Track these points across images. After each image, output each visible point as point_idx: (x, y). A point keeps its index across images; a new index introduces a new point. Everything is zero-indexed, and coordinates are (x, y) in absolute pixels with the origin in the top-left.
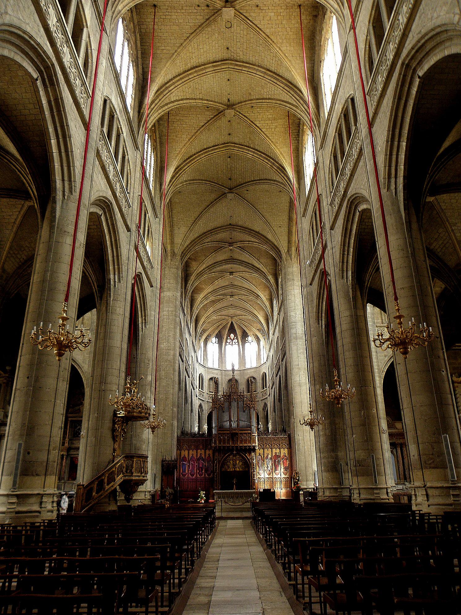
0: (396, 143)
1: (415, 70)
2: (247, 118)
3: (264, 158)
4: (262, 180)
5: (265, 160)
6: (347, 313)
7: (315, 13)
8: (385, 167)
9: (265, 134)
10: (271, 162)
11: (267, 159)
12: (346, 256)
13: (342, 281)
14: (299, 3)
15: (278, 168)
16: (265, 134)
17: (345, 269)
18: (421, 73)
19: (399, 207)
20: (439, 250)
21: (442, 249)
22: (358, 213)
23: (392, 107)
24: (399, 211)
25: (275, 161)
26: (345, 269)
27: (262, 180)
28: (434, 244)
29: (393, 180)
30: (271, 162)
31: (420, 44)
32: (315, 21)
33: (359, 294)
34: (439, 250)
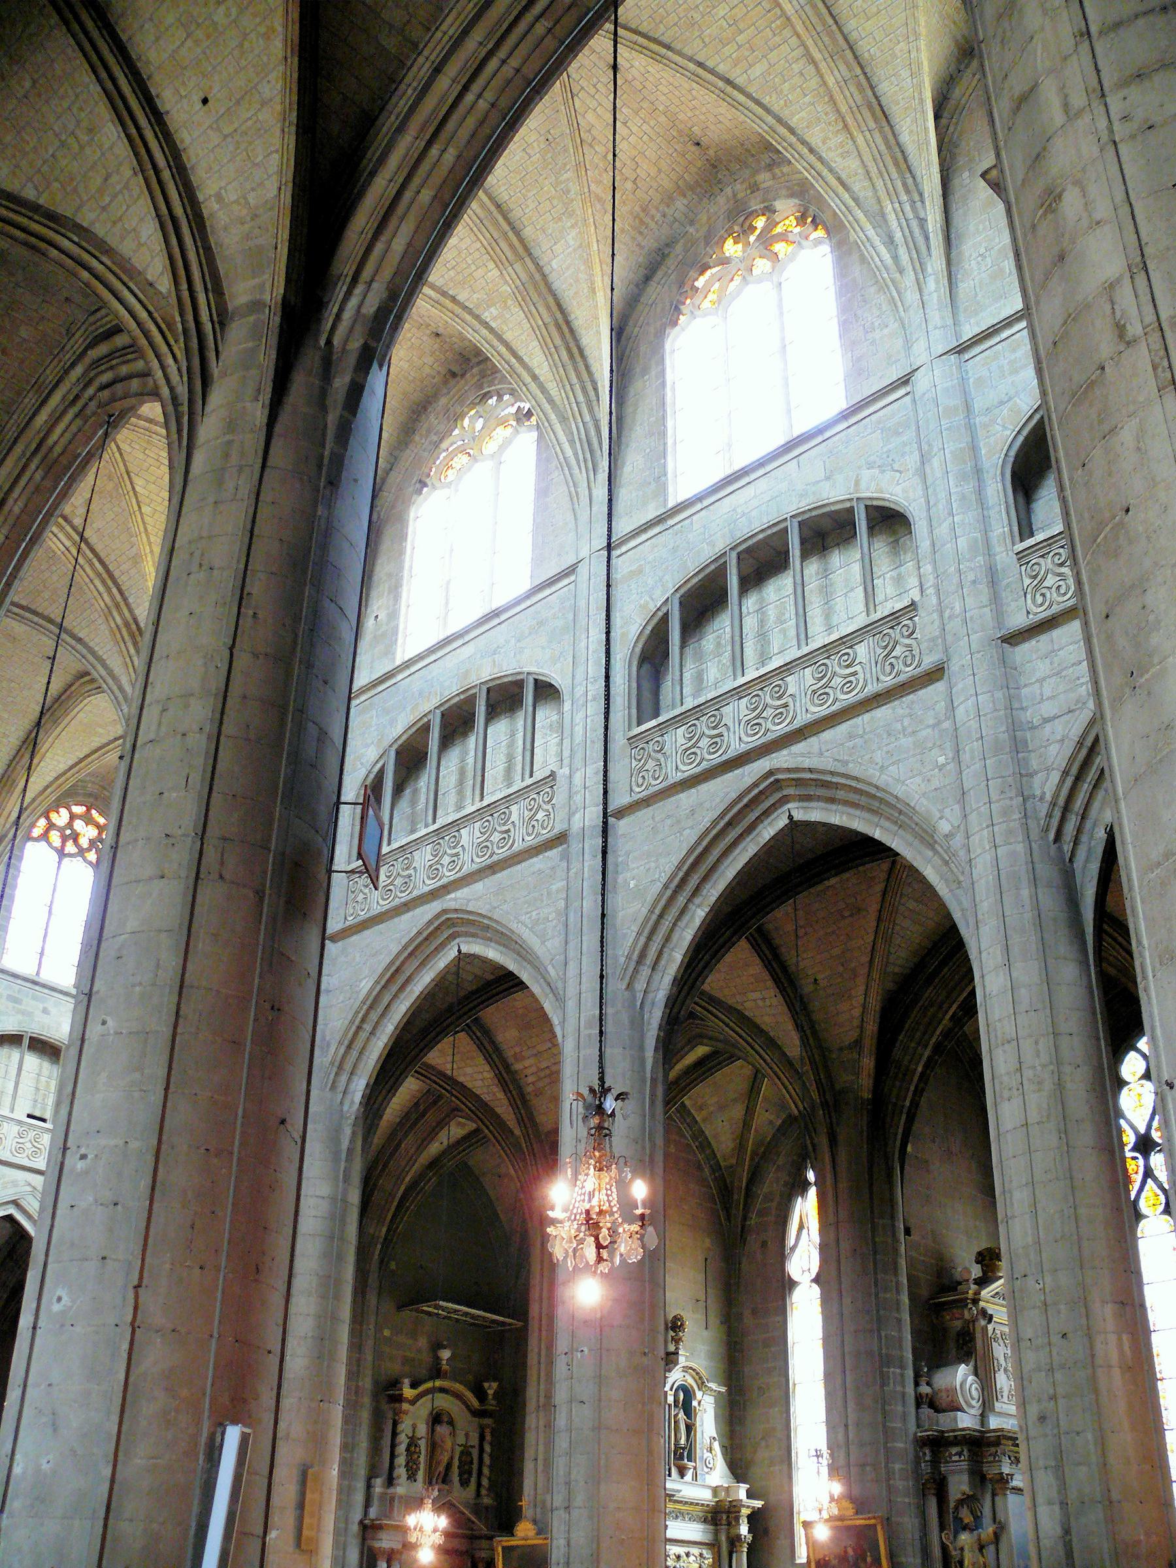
0: (681, 900)
1: (785, 800)
2: (121, 454)
3: (99, 575)
4: (35, 613)
5: (97, 582)
6: (324, 1189)
7: (455, 369)
8: (639, 934)
9: (144, 523)
10: (113, 598)
11: (104, 582)
12: (363, 1035)
13: (328, 1095)
14: (441, 331)
15: (127, 625)
16: (144, 523)
17: (348, 1067)
18: (798, 816)
19: (642, 1037)
20: (530, 1079)
21: (540, 1079)
22: (453, 953)
23: (707, 831)
24: (641, 1048)
25: (125, 600)
26: (348, 1067)
27: (35, 613)
28: (527, 1063)
29: (645, 971)
30: (113, 598)
31: (828, 778)
32: (446, 382)
33: (359, 1143)
34: (530, 1079)
